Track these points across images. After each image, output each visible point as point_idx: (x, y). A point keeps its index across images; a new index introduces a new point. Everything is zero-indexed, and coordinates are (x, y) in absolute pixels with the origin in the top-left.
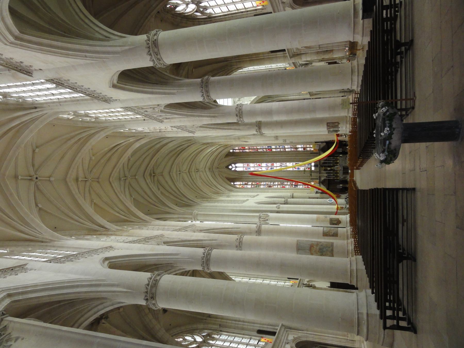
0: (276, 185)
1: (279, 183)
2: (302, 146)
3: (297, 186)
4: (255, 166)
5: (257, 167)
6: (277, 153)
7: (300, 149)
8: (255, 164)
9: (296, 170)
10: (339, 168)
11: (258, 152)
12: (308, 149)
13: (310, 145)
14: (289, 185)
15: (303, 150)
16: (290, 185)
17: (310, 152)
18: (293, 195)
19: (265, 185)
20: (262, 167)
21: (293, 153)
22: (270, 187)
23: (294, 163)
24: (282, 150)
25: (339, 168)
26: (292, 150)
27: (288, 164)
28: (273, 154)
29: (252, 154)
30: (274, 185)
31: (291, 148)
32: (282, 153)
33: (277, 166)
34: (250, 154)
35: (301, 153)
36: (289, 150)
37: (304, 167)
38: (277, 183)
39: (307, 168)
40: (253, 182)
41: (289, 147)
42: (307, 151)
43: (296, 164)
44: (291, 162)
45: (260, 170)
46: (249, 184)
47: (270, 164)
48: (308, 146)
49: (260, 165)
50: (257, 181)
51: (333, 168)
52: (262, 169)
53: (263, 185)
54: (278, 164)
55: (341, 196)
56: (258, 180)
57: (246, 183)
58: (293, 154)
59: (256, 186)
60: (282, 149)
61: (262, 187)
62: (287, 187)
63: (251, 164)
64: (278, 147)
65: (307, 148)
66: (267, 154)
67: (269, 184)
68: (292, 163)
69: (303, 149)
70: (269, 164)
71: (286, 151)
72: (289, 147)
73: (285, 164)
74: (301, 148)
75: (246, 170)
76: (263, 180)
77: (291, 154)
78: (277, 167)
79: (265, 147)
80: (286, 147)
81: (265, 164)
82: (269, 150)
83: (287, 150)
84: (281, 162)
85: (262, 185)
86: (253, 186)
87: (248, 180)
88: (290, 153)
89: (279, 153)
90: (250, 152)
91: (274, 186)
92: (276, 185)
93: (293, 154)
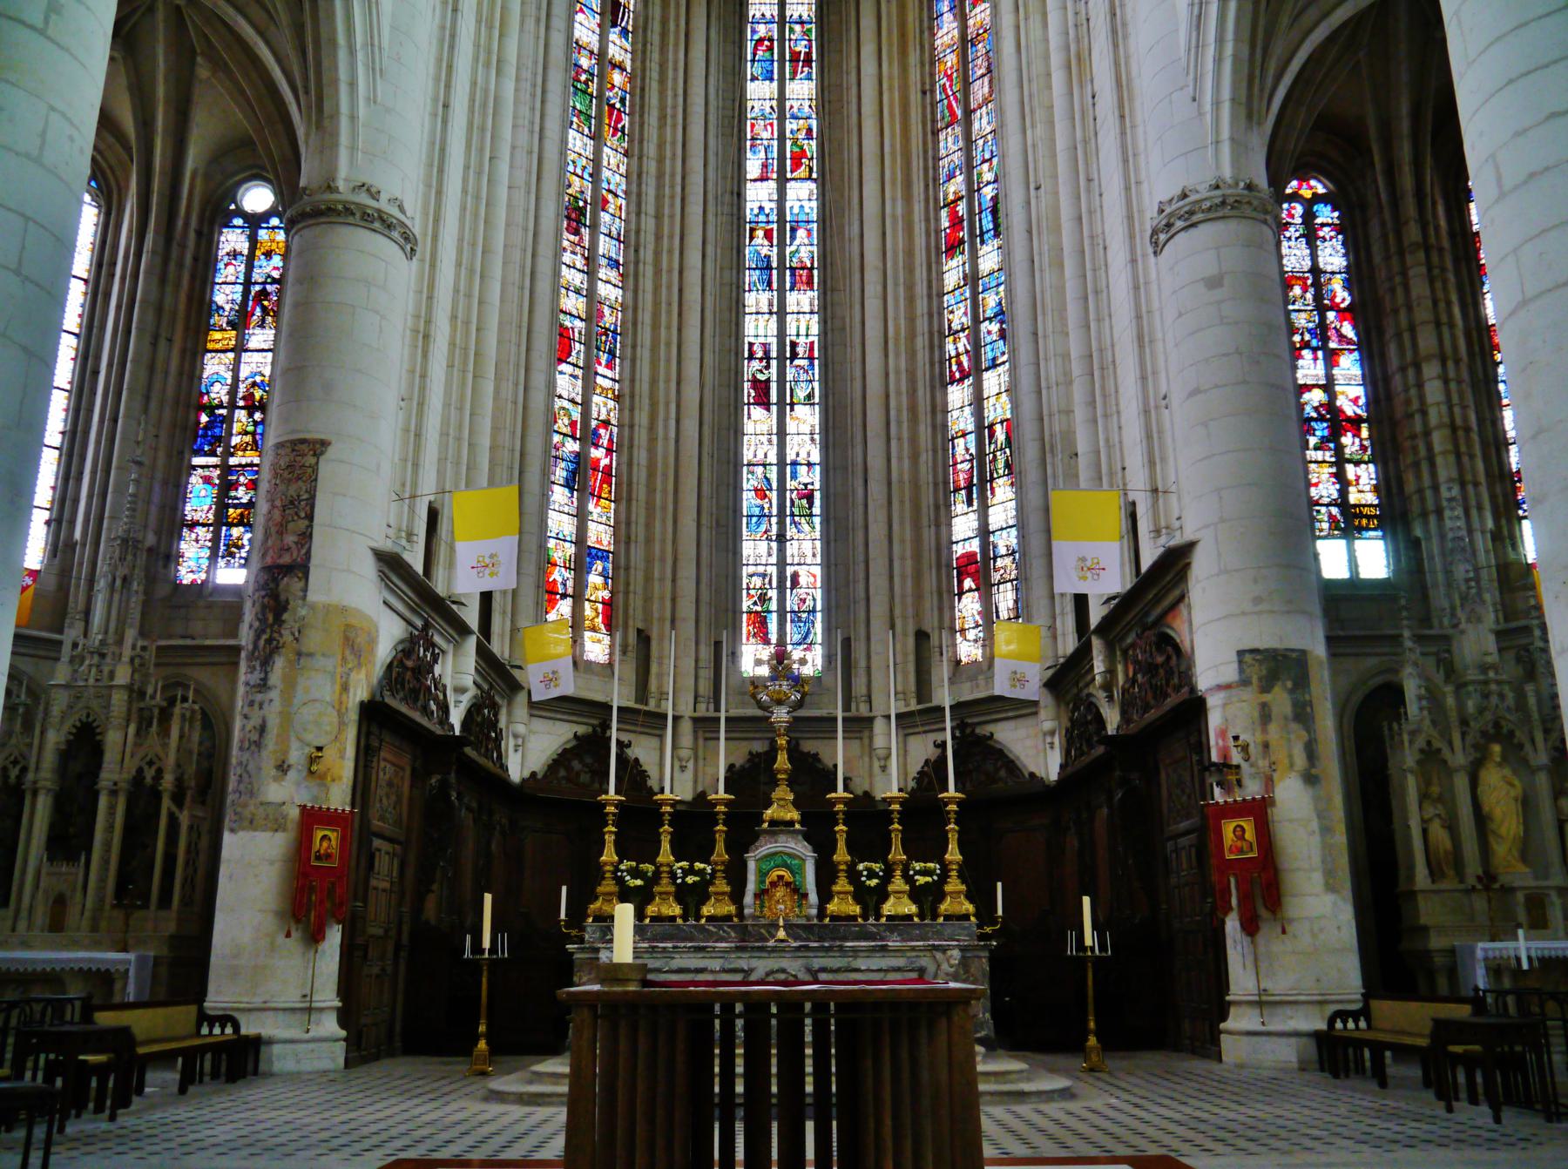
0: (591, 272)
1: (609, 319)
2: (1005, 541)
3: (569, 484)
4: (790, 125)
5: (782, 138)
6: (921, 306)
7: (964, 525)
8: (814, 123)
9: (749, 500)
10: (781, 904)
11: (936, 133)
12: (969, 606)
13: (1018, 612)
14: (586, 405)
15: (959, 550)
16: (586, 414)
17: (930, 624)
18: (382, 223)
19: (596, 176)
20: (782, 182)
21: (925, 458)
22: (576, 217)
23: (812, 478)
24: (957, 346)
25: (781, 904)
26: (963, 448)
27: (805, 419)
28: (910, 269)
29: (914, 75)
30: (591, 260)
31: (983, 429)
32: (922, 357)
33: (789, 318)
34: (913, 58)
35: (928, 535)
36: (961, 420)
37: (773, 570)
38: (609, 292)
39: (763, 599)
40: (631, 79)
41: (998, 409)
42: (948, 597)
43: (810, 497)
44: (825, 448)
45: (753, 167)
46: (614, 35)
47: (804, 253)
48: (1005, 599)
49: (797, 164)
50: (639, 111)
51: (783, 807)
52: (763, 179)
53: (596, 161)
54: (805, 327)
55: (315, 937)
56: (652, 119)
57: (628, 22)
58: (915, 457)
59: (593, 88)
60: (963, 343)
61: (578, 143)
62: (567, 383)
63: (813, 84)
64: (991, 301)
65: (986, 589)
66: (909, 212)
67: (605, 217)
68: (816, 457)
69: (974, 546)
70: (804, 248)
71: (942, 382)
72: (998, 409)
73: (801, 394)
74: (984, 532)
75: (750, 46)
76: (651, 167)
77: (914, 441)
78: (782, 314)
79: (988, 176)
80: (993, 381)
81: (812, 209)
82: (956, 222)
83: (958, 395)
84: (824, 347)
85: (598, 153)
86: (585, 62)
87: (655, 39)
88: (924, 432)
89: (922, 325)
90: (931, 59)
91: (580, 262)
92: (591, 272)
93: (915, 457)
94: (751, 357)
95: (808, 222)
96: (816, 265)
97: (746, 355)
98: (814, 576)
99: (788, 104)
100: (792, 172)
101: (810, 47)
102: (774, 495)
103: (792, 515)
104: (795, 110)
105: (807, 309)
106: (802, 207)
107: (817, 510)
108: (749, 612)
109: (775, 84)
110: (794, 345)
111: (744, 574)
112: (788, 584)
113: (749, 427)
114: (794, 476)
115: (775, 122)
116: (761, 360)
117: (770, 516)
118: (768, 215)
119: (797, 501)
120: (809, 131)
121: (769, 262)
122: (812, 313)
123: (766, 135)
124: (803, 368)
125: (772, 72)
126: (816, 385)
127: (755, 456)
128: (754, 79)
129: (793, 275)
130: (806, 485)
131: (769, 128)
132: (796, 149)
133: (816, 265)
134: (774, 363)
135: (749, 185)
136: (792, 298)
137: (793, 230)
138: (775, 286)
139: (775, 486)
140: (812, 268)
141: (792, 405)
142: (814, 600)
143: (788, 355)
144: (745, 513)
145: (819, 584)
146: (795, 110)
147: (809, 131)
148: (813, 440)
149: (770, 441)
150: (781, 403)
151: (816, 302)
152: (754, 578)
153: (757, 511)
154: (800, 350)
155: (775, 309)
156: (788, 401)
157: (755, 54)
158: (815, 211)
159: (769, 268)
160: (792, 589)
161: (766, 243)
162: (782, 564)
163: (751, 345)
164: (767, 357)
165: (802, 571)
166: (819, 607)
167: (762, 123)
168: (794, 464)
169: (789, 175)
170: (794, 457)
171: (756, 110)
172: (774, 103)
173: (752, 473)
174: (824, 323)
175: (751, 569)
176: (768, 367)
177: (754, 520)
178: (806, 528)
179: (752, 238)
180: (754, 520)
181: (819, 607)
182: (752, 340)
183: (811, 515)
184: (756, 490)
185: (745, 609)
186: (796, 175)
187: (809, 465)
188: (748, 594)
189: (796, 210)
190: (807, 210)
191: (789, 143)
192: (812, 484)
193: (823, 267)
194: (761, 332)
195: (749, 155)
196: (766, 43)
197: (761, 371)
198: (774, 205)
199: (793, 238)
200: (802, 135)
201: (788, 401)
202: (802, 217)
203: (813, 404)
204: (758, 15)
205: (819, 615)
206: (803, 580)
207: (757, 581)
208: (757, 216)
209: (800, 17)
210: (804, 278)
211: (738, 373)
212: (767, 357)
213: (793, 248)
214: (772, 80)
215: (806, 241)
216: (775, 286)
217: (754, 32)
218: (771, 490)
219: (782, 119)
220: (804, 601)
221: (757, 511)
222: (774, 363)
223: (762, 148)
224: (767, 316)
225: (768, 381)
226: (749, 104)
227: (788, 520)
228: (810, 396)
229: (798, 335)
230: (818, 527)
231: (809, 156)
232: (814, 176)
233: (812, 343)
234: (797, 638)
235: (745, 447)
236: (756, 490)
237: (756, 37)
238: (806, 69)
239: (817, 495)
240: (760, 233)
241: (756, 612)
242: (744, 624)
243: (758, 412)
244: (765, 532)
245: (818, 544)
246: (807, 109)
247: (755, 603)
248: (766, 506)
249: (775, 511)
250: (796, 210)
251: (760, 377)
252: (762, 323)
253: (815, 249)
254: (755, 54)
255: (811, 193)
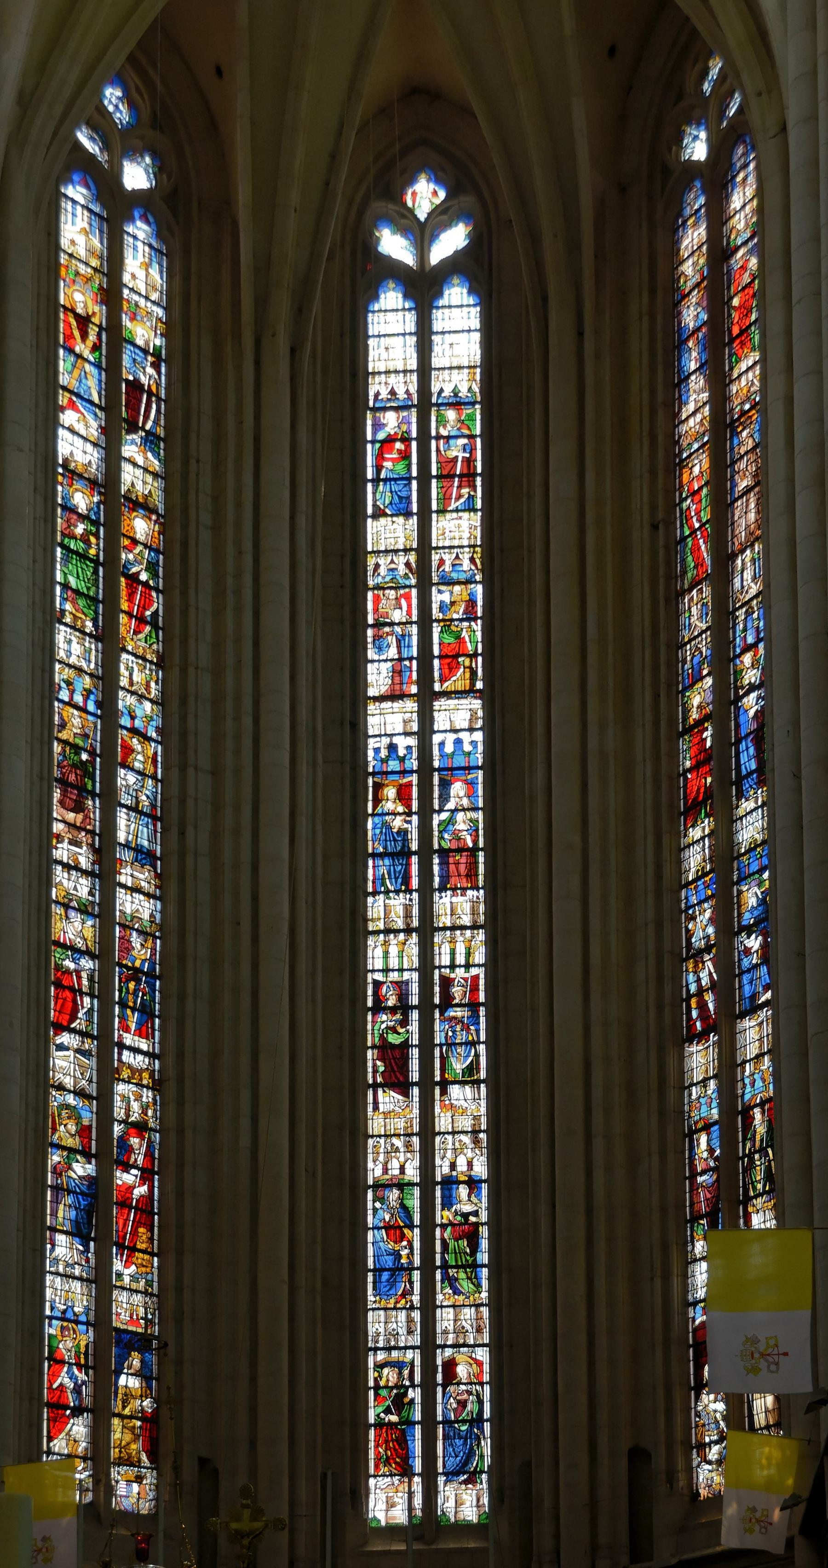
4: (439, 597)
39: (400, 1403)
43: (473, 1238)
52: (393, 696)
63: (476, 519)
68: (481, 1169)
73: (458, 1066)
94: (379, 1007)
95: (468, 769)
96: (481, 844)
97: (370, 1003)
98: (480, 1364)
99: (435, 557)
100: (442, 680)
101: (473, 450)
102: (416, 1235)
103: (445, 1266)
104: (447, 567)
105: (466, 920)
106: (458, 742)
107: (483, 1257)
108: (380, 1425)
109: (414, 521)
110: (446, 983)
111: (371, 1364)
112: (439, 1378)
113: (376, 1125)
114: (447, 1203)
115: (414, 592)
116: (393, 1010)
117: (410, 1269)
118: (402, 760)
119: (452, 1244)
120: (471, 603)
121: (406, 841)
122: (474, 927)
123: (397, 616)
124: (459, 1021)
125: (409, 498)
126: (482, 1048)
127: (385, 1171)
128: (379, 514)
129: (444, 863)
130: (466, 1216)
131: (404, 603)
132: (449, 639)
133: (481, 844)
134: (415, 1015)
135: (372, 708)
136: (443, 902)
137: (445, 785)
138: (415, 883)
139: (417, 1220)
140: (475, 849)
141: (444, 1085)
142: (480, 1402)
143: (437, 1000)
144: (371, 1264)
145: (486, 1378)
146: (447, 567)
147: (471, 603)
148: (476, 1142)
149: (408, 1146)
150: (426, 1084)
151: (482, 908)
152: (386, 1371)
153: (389, 1261)
154: (457, 992)
155: (415, 923)
156: (438, 1078)
157: (379, 468)
158: (480, 748)
159: (406, 853)
160: (445, 1386)
161: (401, 809)
162: (429, 1346)
163: (377, 984)
164: (403, 1007)
165: (462, 1357)
166: (487, 1414)
167: (392, 594)
168: (449, 1182)
169: (437, 687)
170: (446, 1170)
171: (383, 571)
172: (412, 558)
173: (382, 1200)
174: (491, 944)
175: (381, 1356)
176: (404, 1023)
177: (385, 1276)
178: (465, 1285)
179: (377, 801)
180: (385, 1276)
181: (487, 1414)
182: (379, 977)
183: (475, 1266)
184: (388, 1227)
185: (372, 1420)
186: (448, 685)
187: (473, 1183)
188: (377, 1395)
189: (449, 748)
190: (467, 748)
191: (436, 629)
192: (476, 1214)
193: (491, 849)
194: (394, 963)
195: (371, 654)
196: (398, 445)
197: (394, 1030)
198: (412, 741)
199: (445, 798)
200: (458, 613)
201: (438, 1078)
202: (459, 761)
203: (478, 1082)
204: (384, 394)
205: (487, 1426)
206: (462, 1371)
207: (390, 1376)
208: (384, 761)
209: (456, 395)
210: (462, 868)
211: (358, 1032)
212: (403, 1007)
213: (444, 816)
214: (408, 514)
215: (465, 802)
216: (415, 883)
217: (378, 426)
218: (411, 1227)
219: (424, 587)
220: (463, 1404)
221: (389, 1261)
222: (415, 1015)
223: (392, 640)
224: (402, 936)
225: (405, 1045)
226: (371, 561)
227: (438, 1275)
228: (472, 1069)
229: (453, 966)
230: (485, 1284)
231: (470, 647)
232: (479, 685)
233: (476, 978)
234: (452, 1463)
235: (370, 1157)
236: (388, 1227)
237: (381, 436)
238: (465, 491)
239: (484, 1231)
240: (391, 792)
241: (391, 1424)
242: (372, 1444)
243: (388, 1099)
244: (403, 1295)
245: (485, 1311)
246: (466, 565)
247: (387, 1411)
248: (404, 1252)
249: (417, 1261)
250: (449, 748)
251: (393, 1039)
252: (393, 950)
253: (480, 815)
254: (379, 468)
255: (473, 718)
